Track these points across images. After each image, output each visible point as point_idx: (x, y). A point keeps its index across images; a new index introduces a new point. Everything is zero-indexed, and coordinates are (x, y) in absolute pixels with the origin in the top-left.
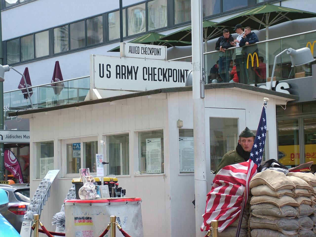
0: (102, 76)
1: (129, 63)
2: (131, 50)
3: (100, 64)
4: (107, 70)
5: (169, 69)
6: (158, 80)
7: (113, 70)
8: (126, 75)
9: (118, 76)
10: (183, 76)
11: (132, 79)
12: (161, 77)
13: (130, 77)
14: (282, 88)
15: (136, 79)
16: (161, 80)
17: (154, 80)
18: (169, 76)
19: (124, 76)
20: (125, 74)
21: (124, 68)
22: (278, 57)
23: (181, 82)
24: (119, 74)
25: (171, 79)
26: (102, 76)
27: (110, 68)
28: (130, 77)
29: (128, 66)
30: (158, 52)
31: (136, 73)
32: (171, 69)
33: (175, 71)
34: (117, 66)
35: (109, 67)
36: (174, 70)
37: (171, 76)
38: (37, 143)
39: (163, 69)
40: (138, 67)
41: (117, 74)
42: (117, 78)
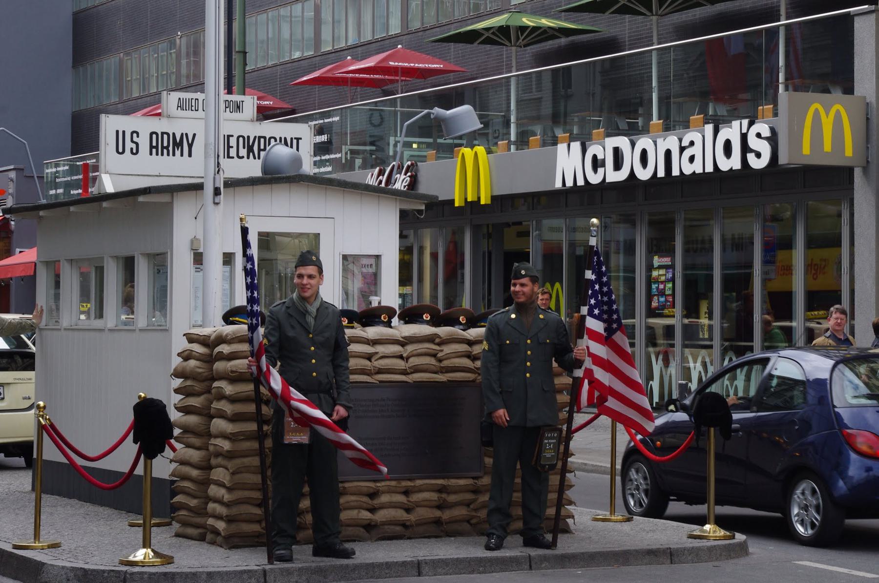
0: (121, 150)
1: (177, 127)
2: (181, 106)
3: (117, 132)
4: (132, 141)
5: (260, 137)
6: (235, 156)
7: (144, 142)
8: (171, 148)
9: (154, 151)
11: (182, 155)
12: (243, 152)
13: (178, 153)
14: (759, 135)
15: (190, 155)
16: (243, 157)
17: (229, 157)
18: (260, 150)
19: (165, 151)
20: (167, 148)
21: (165, 136)
22: (408, 126)
24: (157, 147)
26: (121, 150)
27: (138, 136)
28: (178, 153)
29: (174, 134)
30: (238, 107)
31: (190, 146)
32: (265, 138)
34: (151, 134)
35: (135, 135)
36: (270, 138)
38: (47, 262)
39: (248, 137)
40: (194, 135)
41: (151, 147)
42: (151, 154)
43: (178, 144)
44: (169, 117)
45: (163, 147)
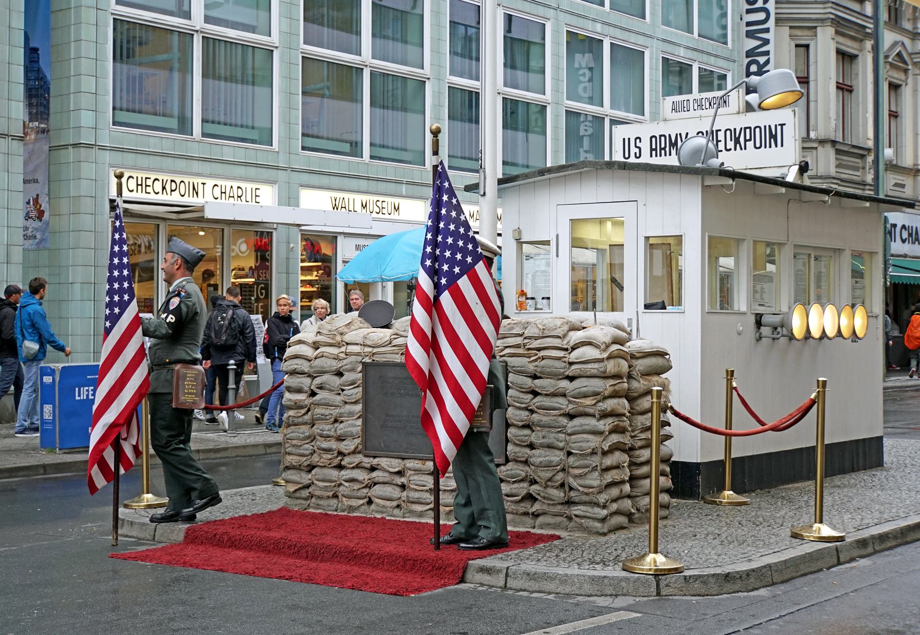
0: (627, 156)
1: (671, 130)
2: (674, 109)
4: (636, 147)
5: (746, 128)
7: (645, 146)
8: (667, 149)
9: (654, 152)
10: (773, 137)
12: (731, 145)
18: (746, 141)
19: (663, 152)
21: (663, 138)
23: (770, 147)
24: (656, 149)
25: (750, 144)
26: (627, 156)
28: (673, 152)
32: (750, 128)
33: (758, 130)
34: (651, 138)
37: (750, 140)
41: (652, 150)
44: (665, 120)
45: (661, 149)
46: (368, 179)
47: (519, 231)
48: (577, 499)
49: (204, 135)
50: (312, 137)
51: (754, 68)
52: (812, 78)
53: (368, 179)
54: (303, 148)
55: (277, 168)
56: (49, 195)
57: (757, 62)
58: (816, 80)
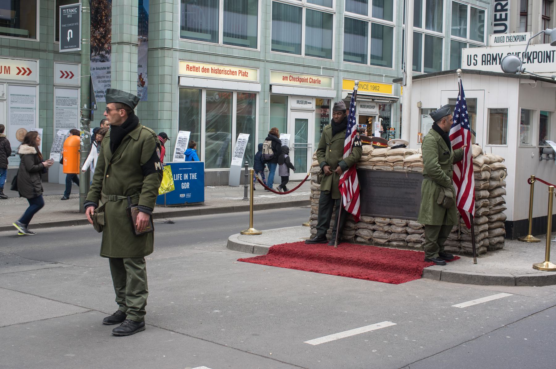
1: (494, 51)
2: (496, 41)
5: (534, 52)
8: (491, 61)
10: (548, 57)
13: (494, 63)
18: (534, 58)
20: (490, 61)
24: (485, 61)
25: (536, 60)
28: (494, 63)
30: (523, 38)
32: (536, 52)
33: (540, 53)
34: (483, 55)
41: (483, 61)
43: (495, 59)
44: (491, 46)
45: (488, 61)
46: (304, 66)
47: (420, 103)
48: (464, 239)
49: (224, 43)
50: (277, 45)
51: (499, 7)
52: (529, 13)
53: (304, 66)
54: (273, 50)
55: (259, 60)
56: (147, 73)
57: (501, 4)
58: (531, 14)
